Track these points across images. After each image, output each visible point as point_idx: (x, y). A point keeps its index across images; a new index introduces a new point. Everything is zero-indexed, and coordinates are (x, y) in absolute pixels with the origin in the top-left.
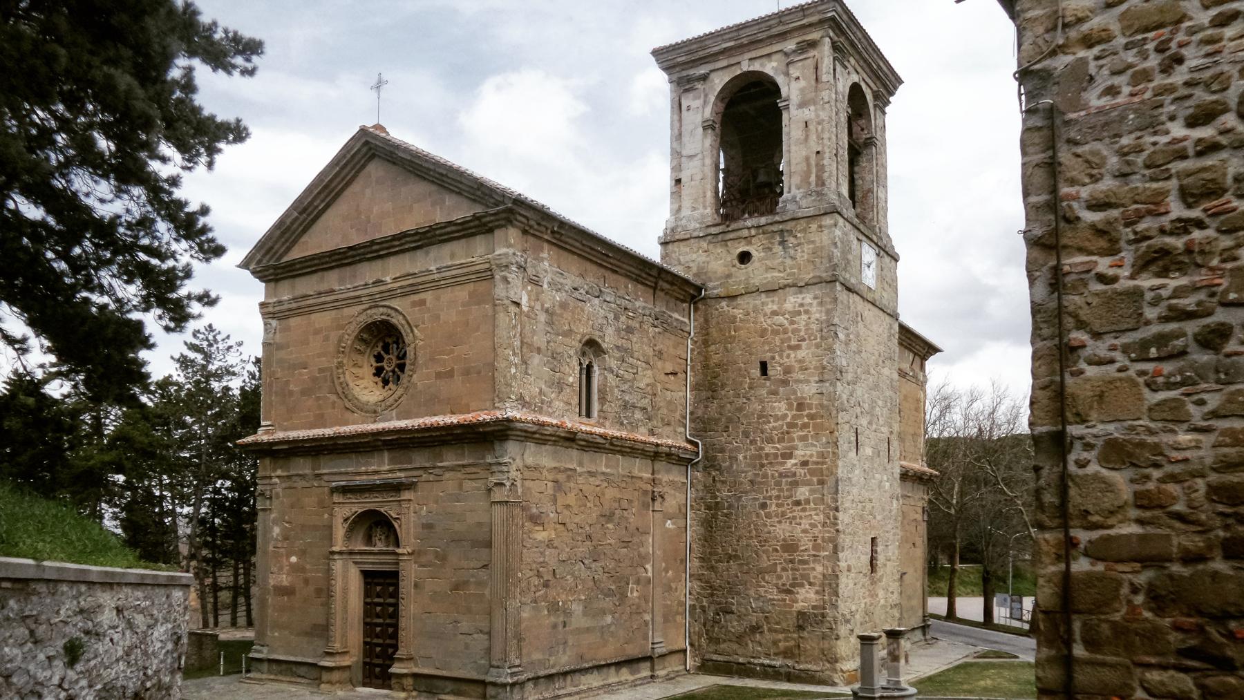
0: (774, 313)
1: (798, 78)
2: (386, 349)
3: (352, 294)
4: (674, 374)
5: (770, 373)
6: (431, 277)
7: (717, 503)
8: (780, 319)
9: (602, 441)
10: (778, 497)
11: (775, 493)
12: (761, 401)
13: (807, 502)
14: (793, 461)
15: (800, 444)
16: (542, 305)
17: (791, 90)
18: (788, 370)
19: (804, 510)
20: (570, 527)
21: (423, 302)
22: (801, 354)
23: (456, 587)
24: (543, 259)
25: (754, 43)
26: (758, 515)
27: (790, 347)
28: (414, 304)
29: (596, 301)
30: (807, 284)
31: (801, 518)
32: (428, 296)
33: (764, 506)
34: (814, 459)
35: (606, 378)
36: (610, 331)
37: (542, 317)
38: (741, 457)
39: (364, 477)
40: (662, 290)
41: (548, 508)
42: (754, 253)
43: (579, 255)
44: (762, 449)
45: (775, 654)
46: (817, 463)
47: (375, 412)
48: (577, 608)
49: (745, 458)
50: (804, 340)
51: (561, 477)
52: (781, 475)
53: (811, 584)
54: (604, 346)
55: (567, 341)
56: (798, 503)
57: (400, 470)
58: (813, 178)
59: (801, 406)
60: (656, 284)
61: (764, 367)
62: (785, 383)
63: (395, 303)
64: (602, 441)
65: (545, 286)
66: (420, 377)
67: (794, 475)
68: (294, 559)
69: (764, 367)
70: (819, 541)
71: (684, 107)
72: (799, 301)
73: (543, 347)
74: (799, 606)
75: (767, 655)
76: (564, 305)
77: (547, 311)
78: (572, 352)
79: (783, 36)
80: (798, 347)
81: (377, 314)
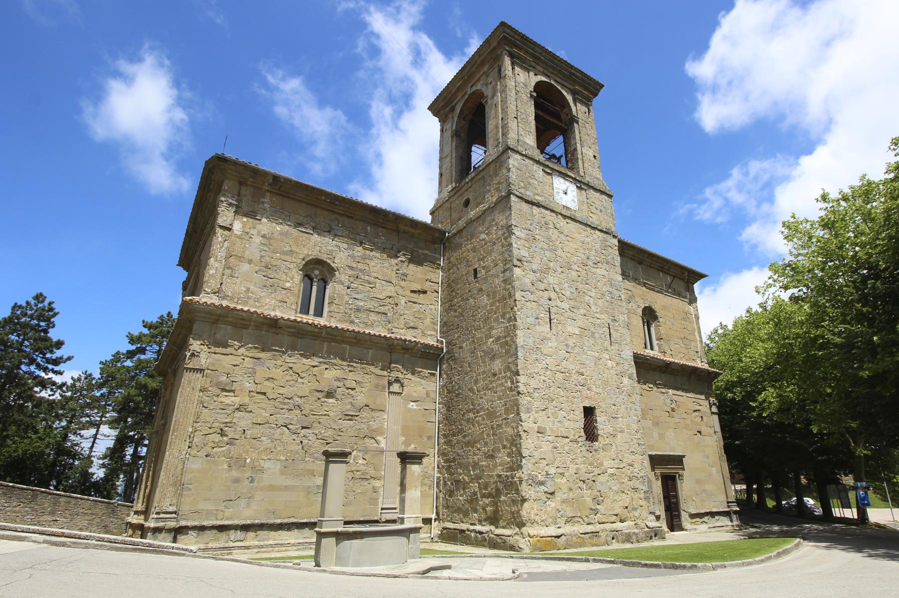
10: (484, 372)
17: (488, 92)
19: (498, 379)
24: (263, 203)
25: (471, 76)
30: (496, 204)
33: (476, 382)
34: (503, 334)
38: (464, 345)
43: (307, 204)
45: (485, 520)
46: (505, 337)
53: (504, 447)
56: (495, 375)
70: (508, 405)
74: (499, 470)
75: (480, 522)
79: (483, 63)
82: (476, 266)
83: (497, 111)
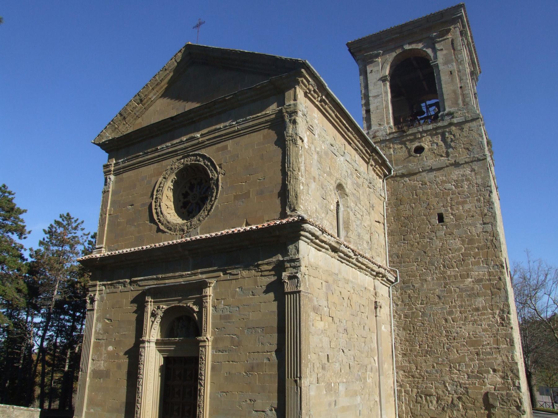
0: (443, 182)
1: (442, 50)
2: (192, 188)
3: (170, 150)
4: (379, 222)
5: (446, 220)
6: (233, 129)
7: (413, 313)
8: (449, 186)
9: (352, 254)
10: (461, 306)
11: (458, 303)
12: (441, 239)
13: (484, 308)
14: (470, 280)
15: (475, 268)
16: (315, 148)
18: (458, 218)
20: (336, 320)
21: (226, 147)
22: (467, 207)
23: (252, 368)
26: (446, 320)
27: (458, 203)
28: (218, 150)
29: (342, 159)
31: (481, 320)
32: (230, 143)
33: (450, 313)
34: (487, 277)
35: (349, 213)
36: (349, 182)
37: (315, 157)
38: (429, 278)
39: (172, 281)
40: (372, 165)
41: (324, 303)
42: (426, 147)
44: (445, 272)
47: (183, 230)
48: (342, 388)
49: (433, 279)
50: (468, 197)
51: (330, 280)
52: (461, 290)
54: (347, 190)
55: (329, 179)
56: (477, 310)
57: (202, 273)
58: (460, 101)
59: (471, 241)
60: (369, 159)
61: (441, 218)
62: (457, 226)
63: (203, 152)
64: (352, 254)
65: (316, 136)
66: (220, 200)
67: (473, 289)
68: (110, 348)
69: (441, 218)
71: (369, 71)
72: (461, 173)
73: (317, 177)
76: (326, 154)
77: (318, 153)
78: (332, 188)
80: (463, 203)
81: (189, 161)
82: (442, 210)
83: (453, 80)
